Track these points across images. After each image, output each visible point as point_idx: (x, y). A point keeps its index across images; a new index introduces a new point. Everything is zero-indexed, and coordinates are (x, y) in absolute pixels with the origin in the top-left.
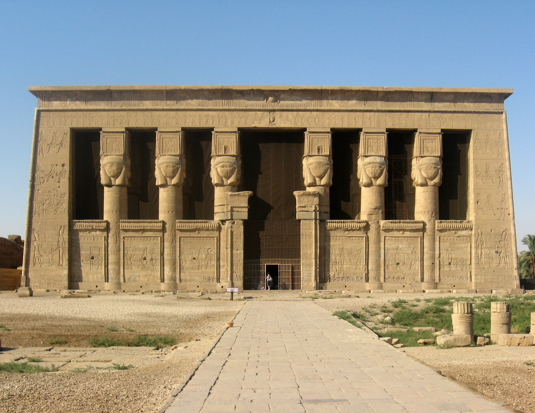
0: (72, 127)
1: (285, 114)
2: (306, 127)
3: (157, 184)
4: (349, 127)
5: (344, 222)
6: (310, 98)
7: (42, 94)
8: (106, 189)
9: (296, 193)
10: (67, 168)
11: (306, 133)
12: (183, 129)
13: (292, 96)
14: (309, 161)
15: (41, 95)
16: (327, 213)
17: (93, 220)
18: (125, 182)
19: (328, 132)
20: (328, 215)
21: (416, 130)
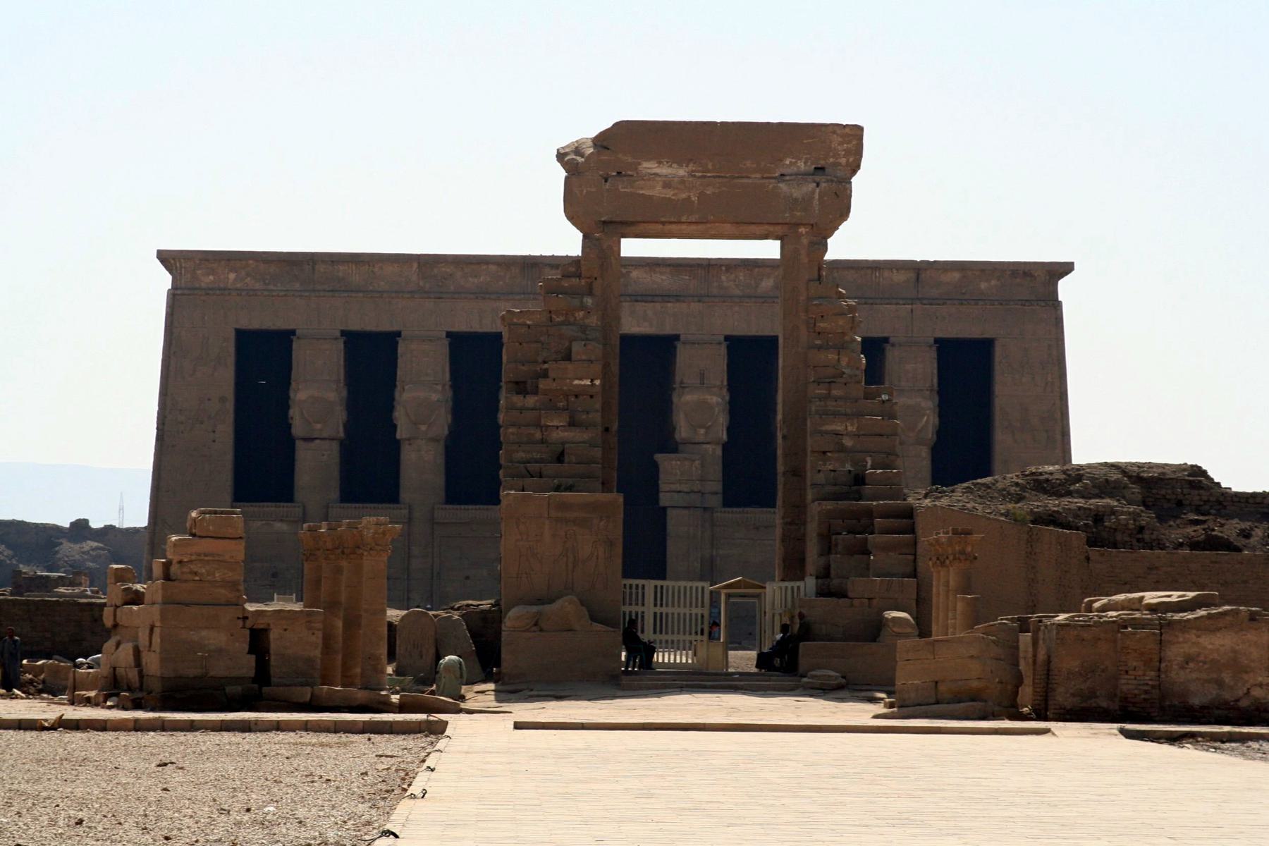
0: (238, 327)
1: (640, 307)
2: (678, 333)
3: (398, 436)
4: (760, 333)
5: (747, 513)
6: (687, 278)
7: (180, 262)
8: (300, 445)
9: (659, 457)
10: (230, 406)
11: (679, 346)
12: (449, 334)
13: (653, 274)
14: (682, 399)
15: (178, 265)
16: (716, 493)
17: (278, 504)
18: (338, 432)
19: (720, 343)
20: (720, 497)
21: (886, 340)
